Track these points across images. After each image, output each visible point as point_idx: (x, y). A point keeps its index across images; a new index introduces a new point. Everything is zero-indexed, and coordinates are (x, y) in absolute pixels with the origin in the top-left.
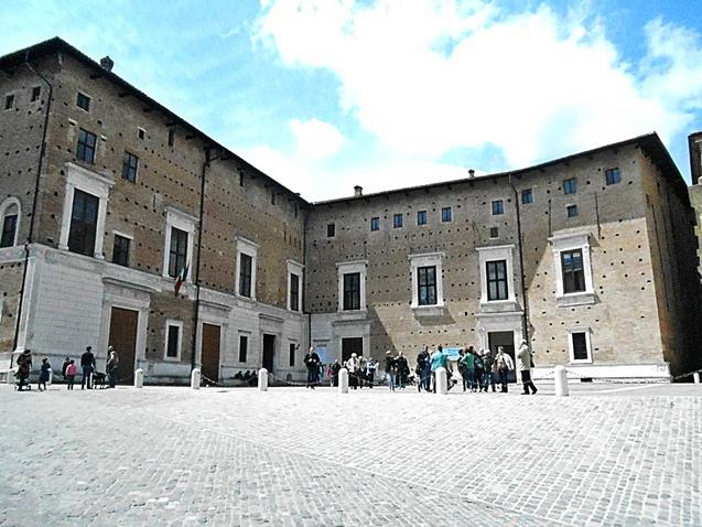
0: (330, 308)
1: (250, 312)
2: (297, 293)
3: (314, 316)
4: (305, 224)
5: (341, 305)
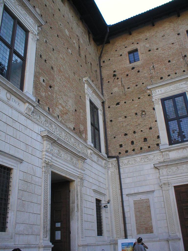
0: (149, 145)
1: (22, 119)
2: (98, 130)
3: (124, 161)
4: (100, 57)
5: (164, 139)
